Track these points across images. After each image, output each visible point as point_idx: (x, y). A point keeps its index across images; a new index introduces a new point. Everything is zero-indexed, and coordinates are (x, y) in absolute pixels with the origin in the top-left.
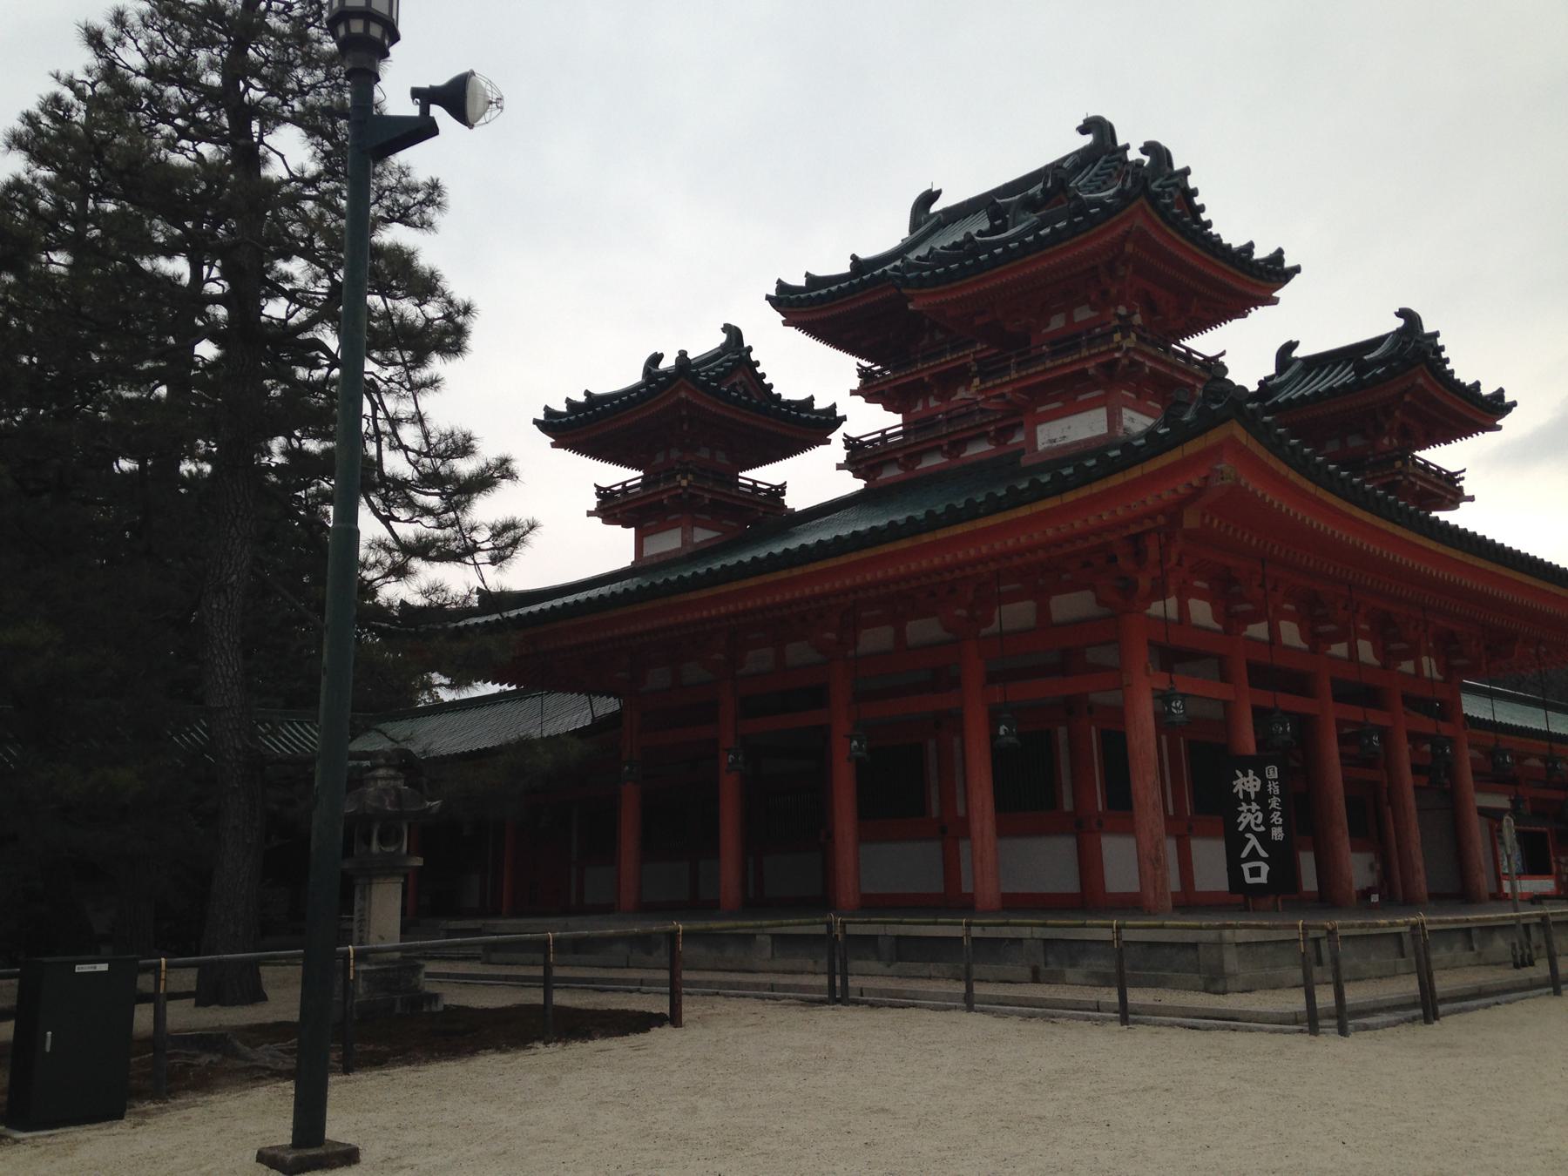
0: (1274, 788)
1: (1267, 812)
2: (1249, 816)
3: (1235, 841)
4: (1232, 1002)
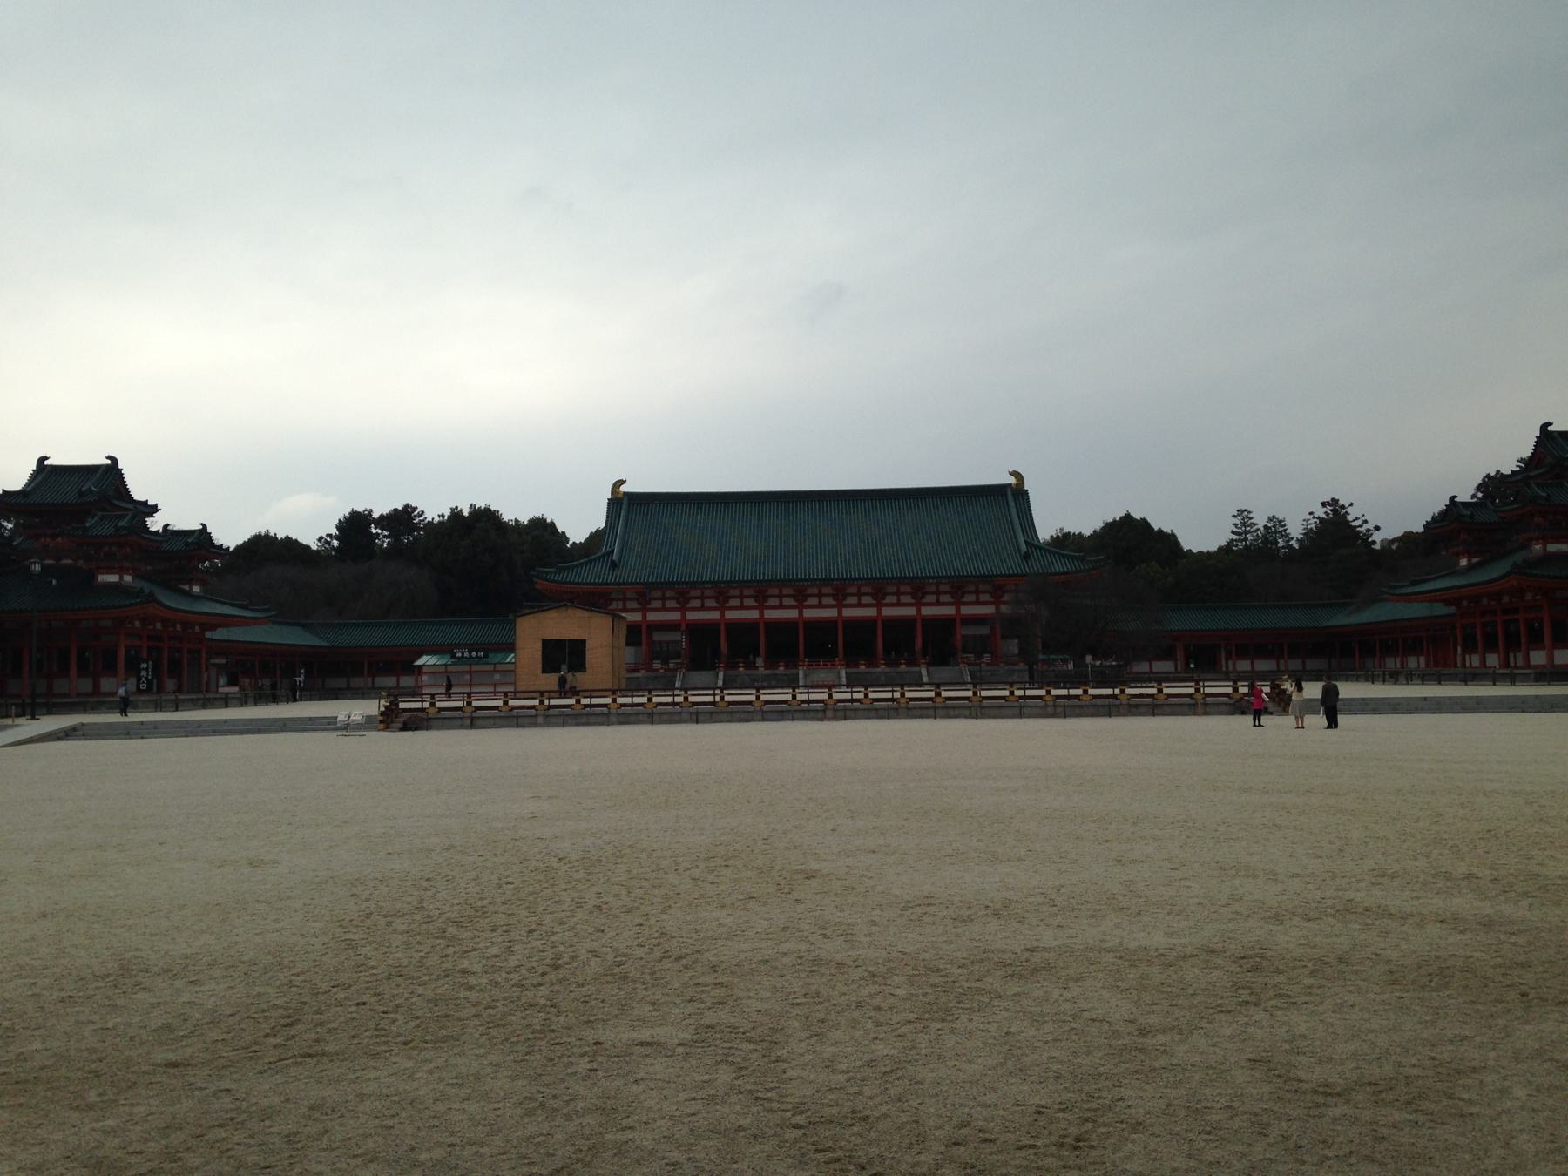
0: (150, 666)
1: (148, 672)
2: (143, 673)
3: (139, 679)
4: (134, 717)
